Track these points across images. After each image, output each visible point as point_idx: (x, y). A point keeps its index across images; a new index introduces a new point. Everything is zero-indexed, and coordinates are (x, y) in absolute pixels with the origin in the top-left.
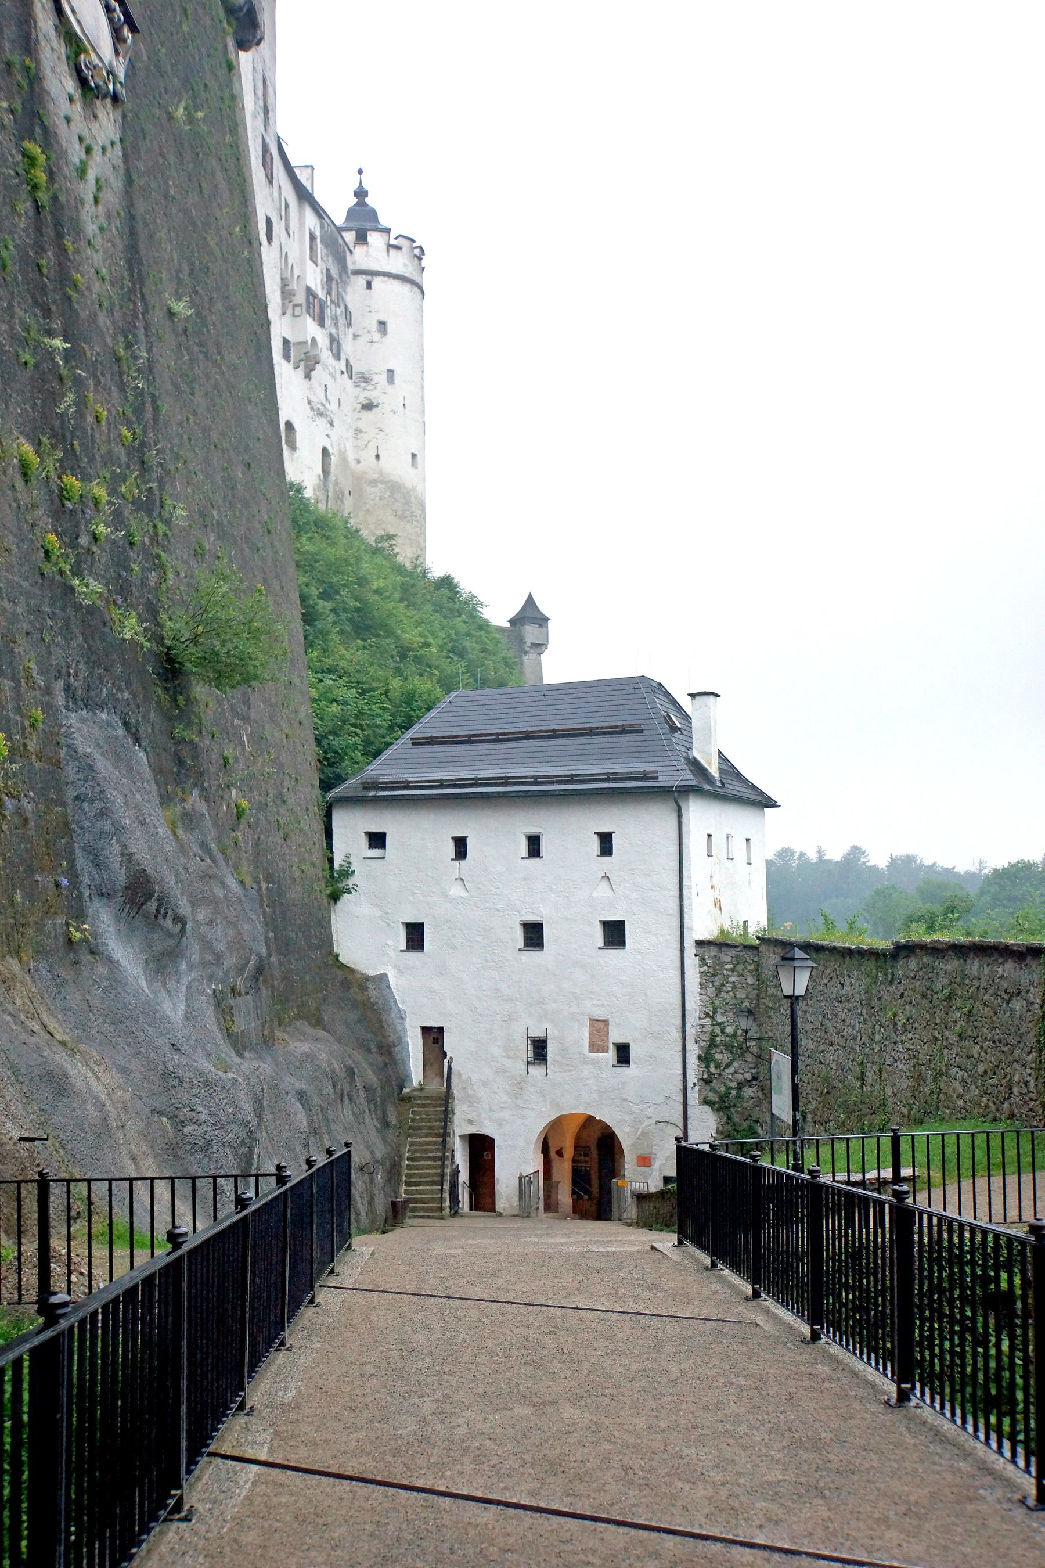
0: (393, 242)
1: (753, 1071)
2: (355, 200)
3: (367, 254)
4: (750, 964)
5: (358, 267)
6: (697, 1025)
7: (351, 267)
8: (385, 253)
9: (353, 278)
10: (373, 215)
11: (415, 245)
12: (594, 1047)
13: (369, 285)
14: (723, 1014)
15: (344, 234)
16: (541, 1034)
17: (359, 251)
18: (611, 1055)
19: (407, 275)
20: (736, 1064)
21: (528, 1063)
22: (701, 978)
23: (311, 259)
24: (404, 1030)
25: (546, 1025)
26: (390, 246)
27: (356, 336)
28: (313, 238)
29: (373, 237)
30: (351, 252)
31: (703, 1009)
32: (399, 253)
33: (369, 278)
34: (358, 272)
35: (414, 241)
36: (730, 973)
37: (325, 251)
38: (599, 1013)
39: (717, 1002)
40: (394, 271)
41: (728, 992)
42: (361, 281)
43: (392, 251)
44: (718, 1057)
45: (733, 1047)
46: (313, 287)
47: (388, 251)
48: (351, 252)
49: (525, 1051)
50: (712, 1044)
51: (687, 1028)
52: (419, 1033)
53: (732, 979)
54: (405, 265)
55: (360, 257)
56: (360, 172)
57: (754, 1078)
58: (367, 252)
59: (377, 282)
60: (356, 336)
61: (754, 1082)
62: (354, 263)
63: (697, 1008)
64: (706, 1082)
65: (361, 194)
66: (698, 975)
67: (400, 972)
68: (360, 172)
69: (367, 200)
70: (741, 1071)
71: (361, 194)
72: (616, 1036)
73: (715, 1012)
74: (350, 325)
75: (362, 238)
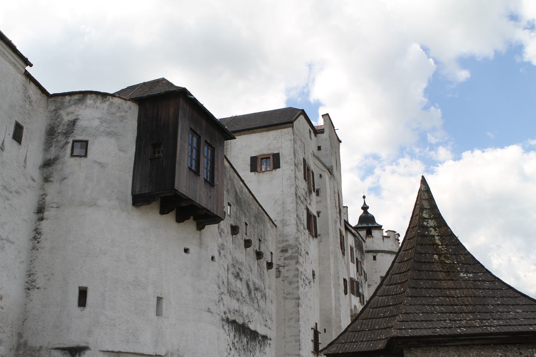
0: (385, 234)
2: (362, 211)
3: (373, 242)
5: (368, 249)
7: (365, 249)
8: (382, 241)
9: (366, 254)
10: (372, 219)
11: (396, 233)
13: (375, 258)
15: (360, 232)
17: (369, 240)
19: (393, 250)
23: (352, 262)
26: (384, 237)
27: (369, 286)
28: (352, 249)
29: (375, 233)
30: (364, 241)
32: (389, 239)
33: (374, 254)
34: (368, 252)
35: (395, 232)
37: (357, 251)
40: (387, 249)
42: (370, 256)
43: (385, 239)
46: (353, 277)
47: (383, 239)
48: (364, 241)
54: (392, 245)
55: (370, 244)
56: (364, 197)
58: (373, 241)
59: (379, 256)
60: (369, 286)
62: (366, 247)
65: (365, 208)
68: (364, 197)
69: (368, 210)
71: (365, 208)
74: (366, 280)
75: (369, 233)
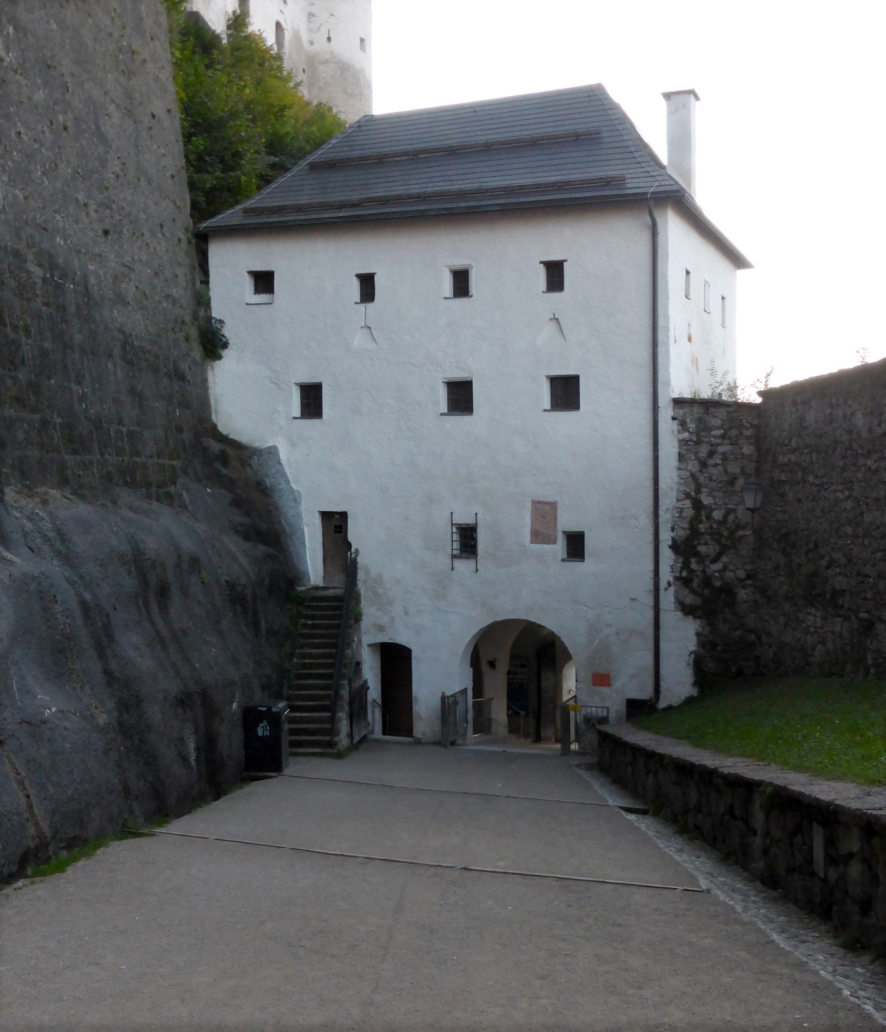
1: (748, 567)
4: (747, 429)
6: (675, 508)
12: (538, 536)
14: (710, 494)
16: (470, 521)
18: (559, 547)
20: (724, 559)
21: (454, 557)
22: (680, 447)
24: (299, 516)
25: (476, 508)
31: (682, 489)
36: (719, 441)
38: (546, 494)
39: (702, 479)
41: (716, 465)
44: (702, 549)
45: (721, 535)
49: (450, 542)
50: (694, 531)
51: (661, 512)
52: (318, 520)
53: (721, 449)
57: (749, 576)
61: (749, 582)
63: (675, 486)
64: (684, 581)
66: (676, 444)
67: (293, 445)
70: (731, 567)
72: (566, 522)
73: (698, 490)
